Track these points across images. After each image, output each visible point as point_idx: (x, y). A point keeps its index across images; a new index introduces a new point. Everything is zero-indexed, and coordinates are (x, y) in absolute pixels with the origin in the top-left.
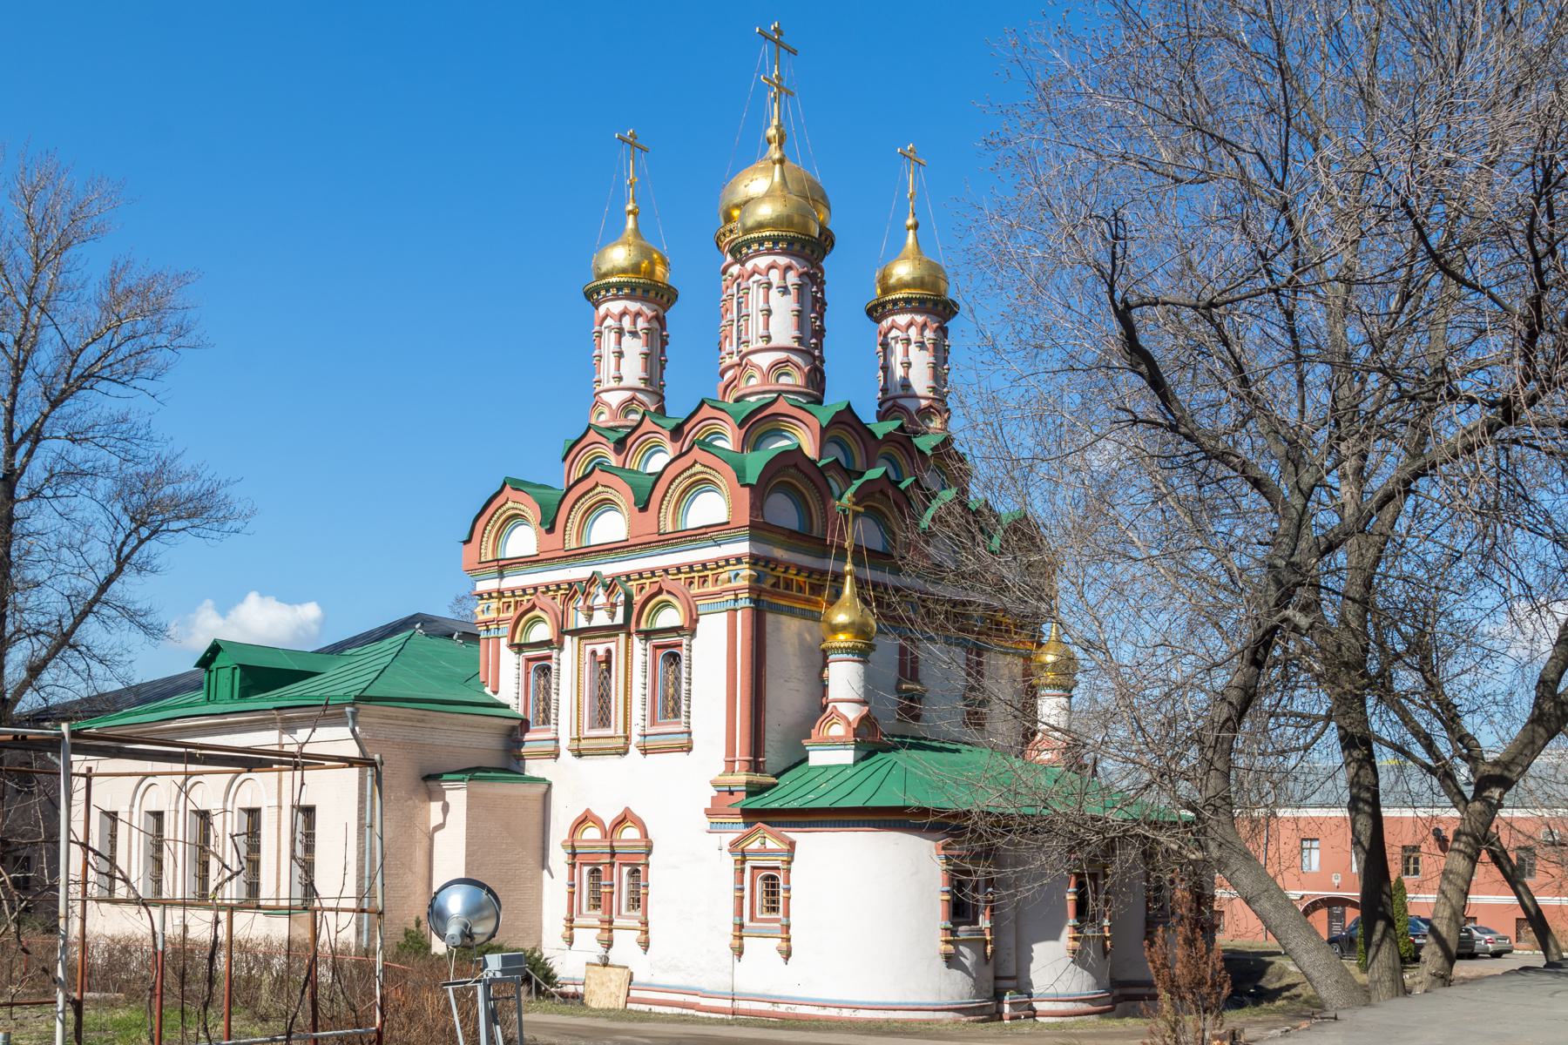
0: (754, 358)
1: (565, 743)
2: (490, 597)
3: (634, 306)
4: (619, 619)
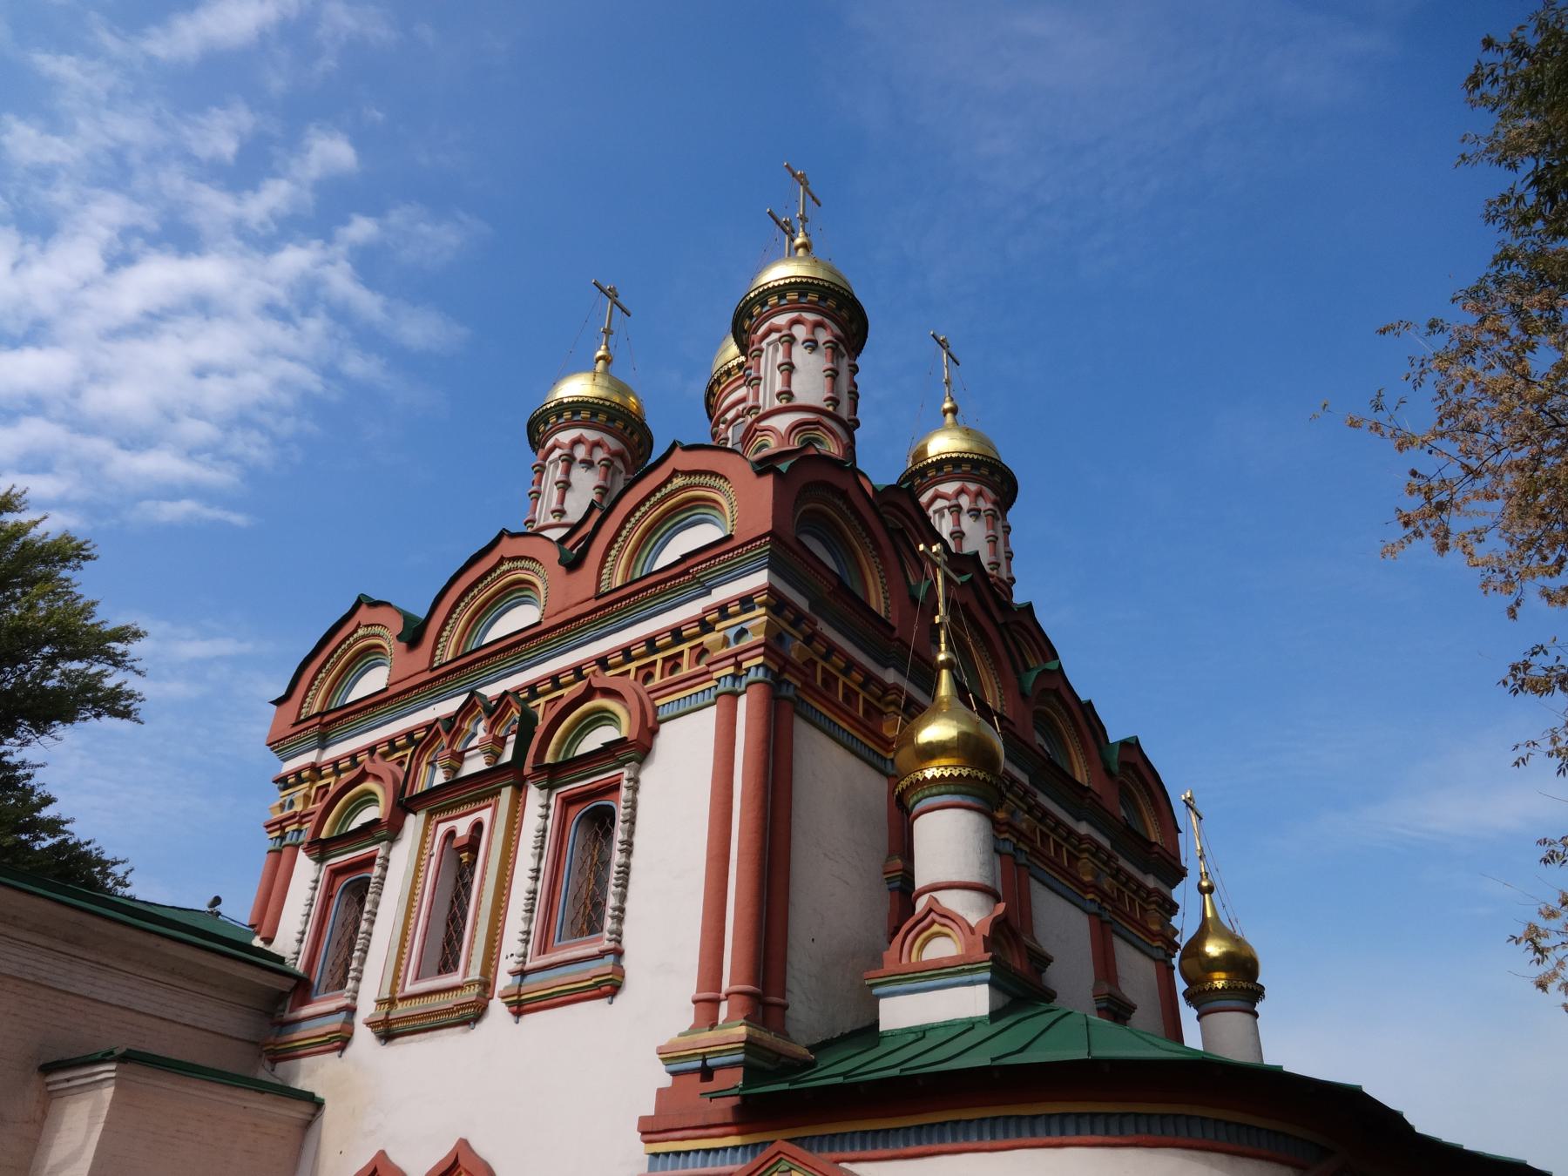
0: (764, 424)
1: (367, 1008)
2: (300, 781)
3: (591, 435)
4: (507, 756)
